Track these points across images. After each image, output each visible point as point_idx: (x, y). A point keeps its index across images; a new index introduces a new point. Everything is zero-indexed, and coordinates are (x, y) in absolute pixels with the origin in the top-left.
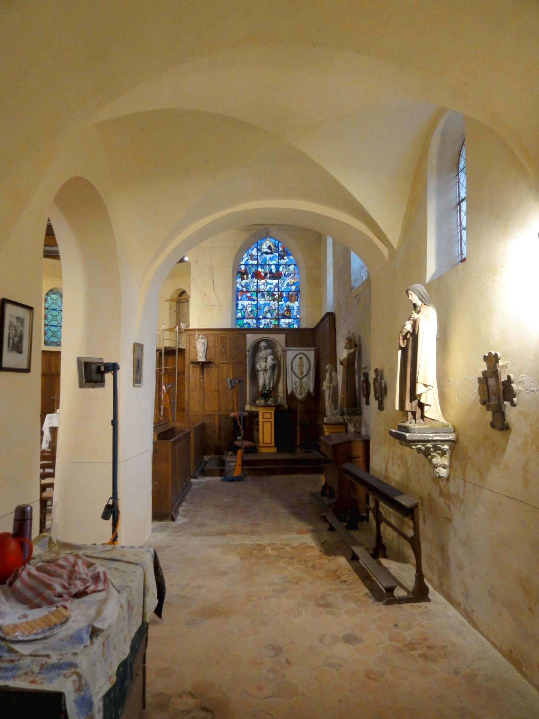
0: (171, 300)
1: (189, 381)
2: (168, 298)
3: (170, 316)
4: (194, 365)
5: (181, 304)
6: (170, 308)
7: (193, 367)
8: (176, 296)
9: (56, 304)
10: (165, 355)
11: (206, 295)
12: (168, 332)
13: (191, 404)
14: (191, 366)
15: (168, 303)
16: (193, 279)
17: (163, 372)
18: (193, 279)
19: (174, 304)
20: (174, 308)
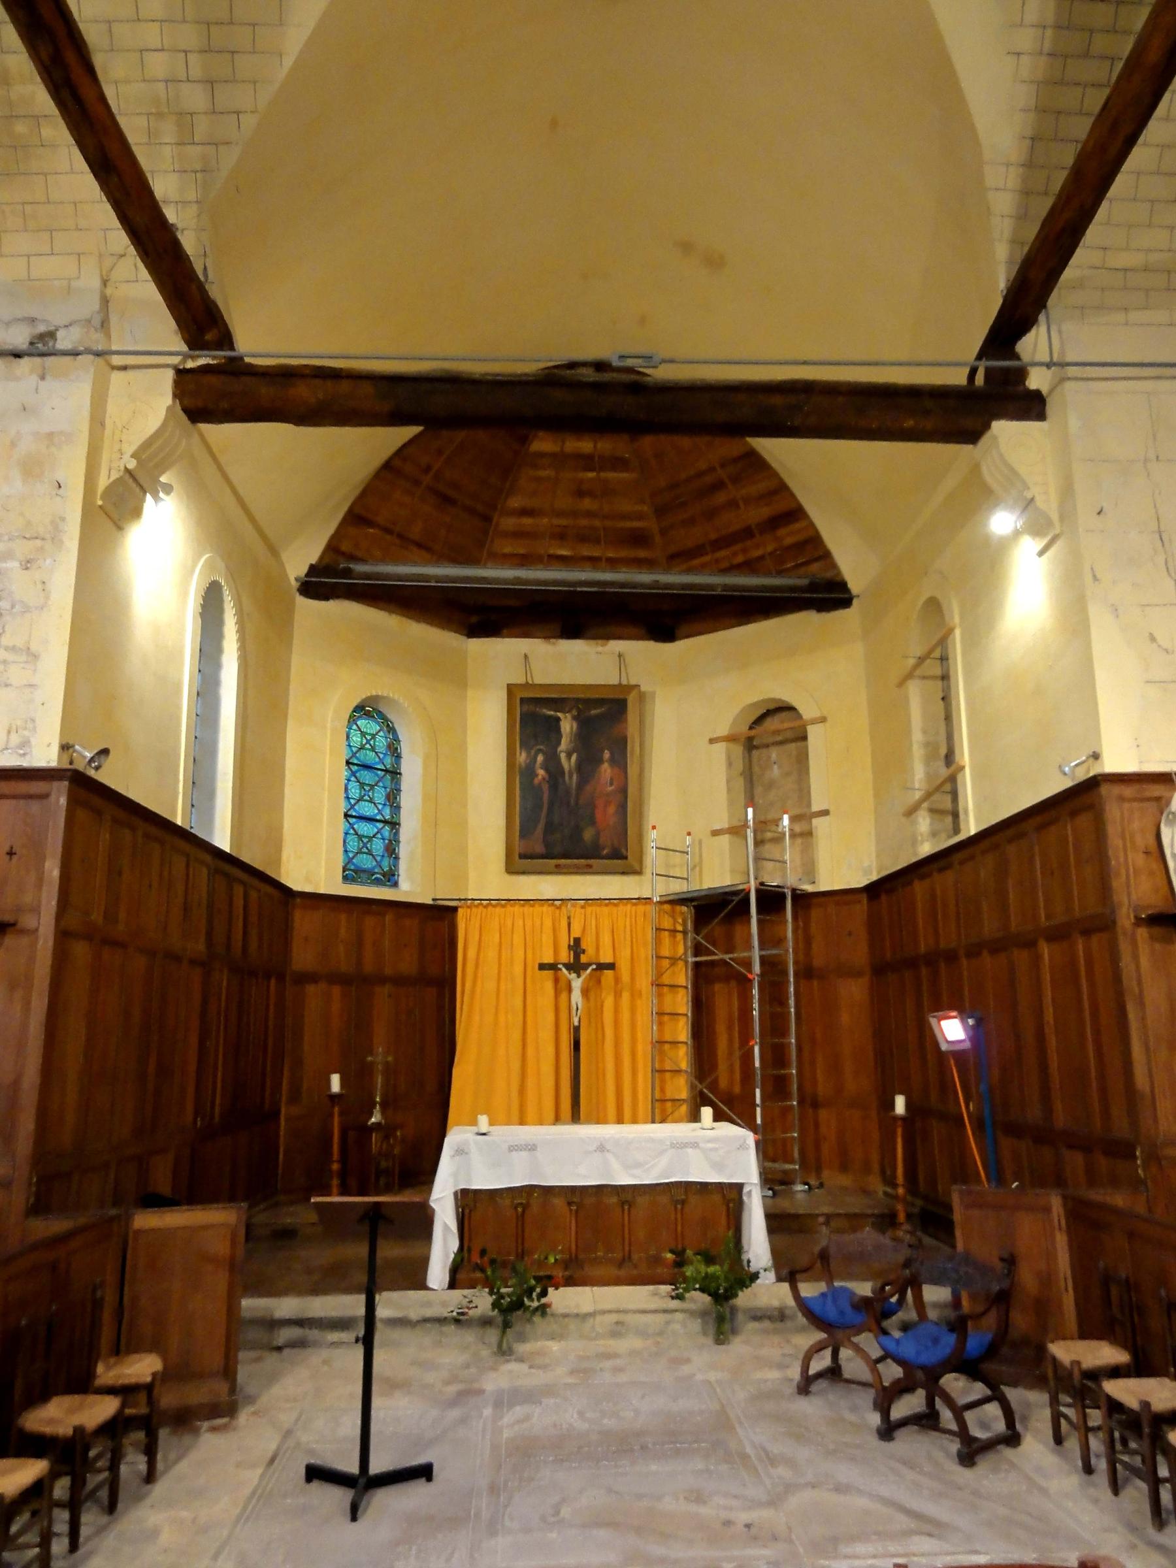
0: (731, 739)
1: (1141, 1004)
2: (723, 730)
3: (729, 790)
4: (1157, 931)
5: (755, 753)
6: (730, 764)
7: (1152, 938)
8: (744, 729)
9: (373, 749)
10: (759, 912)
11: (1153, 639)
12: (725, 838)
13: (1164, 1106)
14: (1142, 933)
15: (721, 747)
16: (1095, 578)
17: (757, 968)
18: (1095, 578)
19: (738, 750)
20: (739, 765)
